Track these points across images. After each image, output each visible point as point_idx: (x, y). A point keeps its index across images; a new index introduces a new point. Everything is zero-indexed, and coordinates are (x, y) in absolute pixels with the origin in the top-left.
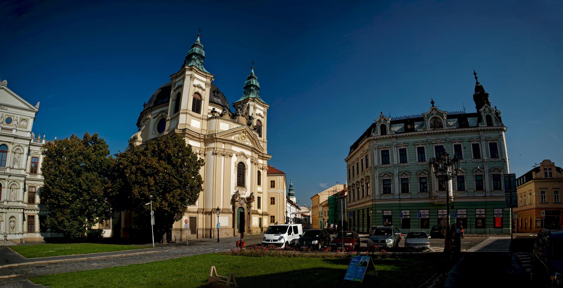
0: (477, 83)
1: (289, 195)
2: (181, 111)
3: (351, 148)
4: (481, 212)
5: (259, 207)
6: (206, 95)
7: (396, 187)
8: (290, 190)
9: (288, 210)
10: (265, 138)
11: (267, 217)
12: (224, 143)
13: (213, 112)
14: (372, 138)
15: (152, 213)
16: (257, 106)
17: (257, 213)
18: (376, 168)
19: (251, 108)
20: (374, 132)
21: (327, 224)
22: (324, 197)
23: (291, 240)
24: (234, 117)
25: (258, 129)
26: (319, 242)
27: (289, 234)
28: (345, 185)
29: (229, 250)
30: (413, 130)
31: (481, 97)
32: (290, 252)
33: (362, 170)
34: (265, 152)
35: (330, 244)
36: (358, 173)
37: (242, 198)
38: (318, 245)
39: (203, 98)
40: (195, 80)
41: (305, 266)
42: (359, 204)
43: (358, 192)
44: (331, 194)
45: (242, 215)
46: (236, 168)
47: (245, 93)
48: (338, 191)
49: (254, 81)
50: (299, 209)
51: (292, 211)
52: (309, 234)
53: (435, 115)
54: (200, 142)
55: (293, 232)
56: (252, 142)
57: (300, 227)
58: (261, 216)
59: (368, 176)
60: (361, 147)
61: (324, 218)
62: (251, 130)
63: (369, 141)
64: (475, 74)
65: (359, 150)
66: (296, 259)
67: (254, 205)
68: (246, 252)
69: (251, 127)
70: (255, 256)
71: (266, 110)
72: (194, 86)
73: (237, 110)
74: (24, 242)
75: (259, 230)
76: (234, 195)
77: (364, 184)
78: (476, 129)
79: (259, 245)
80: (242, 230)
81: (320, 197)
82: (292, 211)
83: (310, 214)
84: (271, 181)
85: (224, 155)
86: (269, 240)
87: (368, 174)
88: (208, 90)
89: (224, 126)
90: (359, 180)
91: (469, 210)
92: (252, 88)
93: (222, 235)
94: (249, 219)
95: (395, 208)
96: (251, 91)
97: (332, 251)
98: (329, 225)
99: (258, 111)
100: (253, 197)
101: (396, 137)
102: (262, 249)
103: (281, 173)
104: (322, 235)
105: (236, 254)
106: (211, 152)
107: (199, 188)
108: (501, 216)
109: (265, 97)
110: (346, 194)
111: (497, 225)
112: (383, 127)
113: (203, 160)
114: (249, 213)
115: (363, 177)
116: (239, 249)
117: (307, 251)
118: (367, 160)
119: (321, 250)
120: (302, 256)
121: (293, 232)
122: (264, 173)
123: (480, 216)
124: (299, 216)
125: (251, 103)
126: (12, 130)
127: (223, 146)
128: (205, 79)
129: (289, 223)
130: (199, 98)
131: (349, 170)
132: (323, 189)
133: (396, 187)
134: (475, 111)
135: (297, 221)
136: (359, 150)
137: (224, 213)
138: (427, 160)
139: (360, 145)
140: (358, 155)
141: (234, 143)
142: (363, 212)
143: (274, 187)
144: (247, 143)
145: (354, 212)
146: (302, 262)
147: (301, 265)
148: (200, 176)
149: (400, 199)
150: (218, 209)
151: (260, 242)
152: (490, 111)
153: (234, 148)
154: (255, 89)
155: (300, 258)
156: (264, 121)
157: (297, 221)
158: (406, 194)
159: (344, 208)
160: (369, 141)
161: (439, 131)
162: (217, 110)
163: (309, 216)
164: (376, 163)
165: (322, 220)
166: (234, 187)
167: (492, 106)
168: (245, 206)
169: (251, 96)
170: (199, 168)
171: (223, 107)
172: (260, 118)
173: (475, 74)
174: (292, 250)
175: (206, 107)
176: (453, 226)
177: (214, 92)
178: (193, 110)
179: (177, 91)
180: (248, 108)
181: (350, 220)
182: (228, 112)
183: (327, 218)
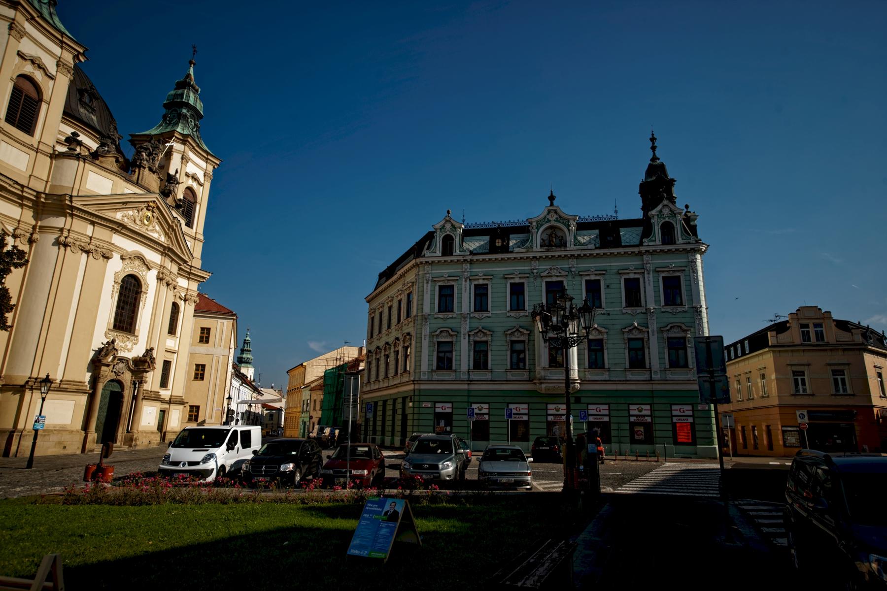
0: (654, 158)
1: (240, 361)
3: (381, 276)
4: (640, 411)
5: (164, 384)
6: (56, 92)
7: (463, 356)
8: (243, 351)
9: (234, 395)
10: (201, 230)
11: (181, 407)
12: (93, 223)
13: (72, 140)
14: (423, 260)
16: (191, 155)
17: (157, 398)
18: (425, 318)
19: (176, 159)
20: (428, 249)
21: (317, 426)
22: (315, 370)
23: (232, 461)
24: (128, 168)
25: (187, 208)
26: (297, 466)
27: (230, 447)
28: (361, 349)
29: (58, 489)
30: (505, 249)
31: (657, 186)
32: (227, 491)
33: (399, 320)
34: (197, 263)
35: (321, 471)
36: (389, 327)
37: (121, 360)
38: (293, 473)
39: (46, 97)
41: (259, 524)
42: (387, 388)
43: (387, 364)
44: (332, 365)
45: (115, 400)
46: (117, 288)
47: (165, 117)
48: (346, 359)
49: (192, 95)
50: (259, 393)
51: (241, 398)
52: (277, 448)
53: (553, 223)
54: (22, 206)
55: (239, 444)
56: (166, 234)
57: (256, 432)
58: (166, 406)
59: (408, 334)
60: (401, 276)
61: (313, 413)
62: (169, 206)
63: (416, 265)
64: (653, 139)
65: (395, 281)
66: (239, 507)
67: (152, 380)
68: (110, 493)
69: (170, 200)
70: (133, 504)
71: (210, 169)
72: (20, 55)
73: (139, 153)
75: (157, 438)
76: (101, 350)
77: (400, 348)
78: (636, 250)
79: (149, 474)
80: (108, 435)
81: (308, 369)
82: (241, 398)
83: (282, 404)
84: (203, 329)
85: (88, 252)
86: (177, 463)
87: (410, 329)
88: (63, 82)
89: (99, 182)
90: (391, 340)
91: (613, 407)
92: (184, 111)
93: (46, 448)
94: (135, 411)
95: (458, 399)
96: (180, 117)
97: (323, 487)
98: (321, 430)
99: (191, 168)
100: (153, 360)
101: (471, 262)
102: (155, 484)
103: (226, 313)
105: (77, 501)
106: (52, 237)
108: (691, 420)
110: (362, 366)
111: (682, 437)
112: (448, 242)
113: (21, 254)
114: (135, 398)
115: (399, 336)
116: (91, 485)
117: (266, 488)
118: (409, 302)
119: (299, 486)
120: (254, 501)
121: (239, 444)
122: (187, 311)
123: (640, 420)
124: (257, 409)
125: (177, 146)
127: (89, 230)
128: (57, 50)
129: (233, 423)
131: (373, 319)
132: (316, 355)
133: (463, 356)
134: (639, 215)
135: (251, 418)
136: (395, 281)
137: (65, 391)
138: (528, 307)
139: (399, 273)
140: (392, 292)
141: (119, 228)
142: (394, 404)
143: (207, 342)
144: (155, 236)
145: (376, 403)
146: (254, 514)
147: (249, 523)
148: (5, 291)
149: (470, 382)
150: (47, 380)
151: (153, 468)
152: (673, 214)
153: (119, 240)
154: (192, 116)
155: (249, 506)
156: (203, 194)
157: (251, 418)
158: (482, 372)
159: (355, 395)
160: (416, 265)
161: (556, 254)
162: (82, 138)
163: (280, 410)
164: (427, 310)
165: (306, 420)
166: (105, 329)
167: (680, 205)
169: (179, 129)
170: (8, 271)
171: (103, 137)
172: (195, 185)
173: (653, 139)
174: (233, 486)
175: (52, 125)
176: (580, 437)
177: (81, 92)
178: (10, 119)
180: (169, 154)
181: (367, 420)
182: (113, 152)
183: (317, 415)
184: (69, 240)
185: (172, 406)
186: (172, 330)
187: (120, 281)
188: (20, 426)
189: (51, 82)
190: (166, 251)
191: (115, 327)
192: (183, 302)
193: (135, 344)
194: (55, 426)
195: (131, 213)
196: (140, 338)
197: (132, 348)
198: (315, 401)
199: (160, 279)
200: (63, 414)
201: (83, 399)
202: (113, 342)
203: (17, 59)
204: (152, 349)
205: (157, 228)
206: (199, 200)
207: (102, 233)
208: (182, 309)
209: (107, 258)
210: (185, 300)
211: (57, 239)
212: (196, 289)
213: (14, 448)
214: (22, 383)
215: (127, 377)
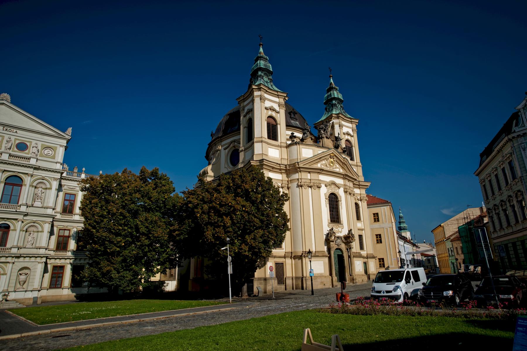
1: (400, 229)
2: (255, 140)
3: (482, 155)
5: (362, 248)
6: (281, 118)
8: (400, 223)
9: (402, 250)
10: (359, 160)
11: (374, 260)
12: (309, 172)
13: (292, 137)
14: (515, 135)
15: (229, 259)
16: (343, 123)
17: (360, 256)
19: (337, 127)
20: (517, 125)
21: (462, 265)
22: (451, 228)
23: (411, 290)
24: (317, 140)
25: (348, 151)
26: (454, 293)
27: (407, 282)
28: (481, 209)
29: (327, 306)
32: (412, 308)
33: (507, 183)
34: (362, 179)
35: (475, 296)
36: (500, 189)
37: (338, 237)
38: (453, 298)
39: (278, 122)
40: (266, 102)
41: (437, 329)
42: (512, 233)
43: (507, 216)
44: (462, 223)
45: (340, 258)
46: (327, 201)
47: (326, 109)
48: (472, 217)
49: (335, 92)
50: (417, 247)
51: (407, 251)
52: (437, 282)
54: (281, 173)
55: (412, 280)
56: (342, 168)
57: (421, 271)
59: (519, 191)
60: (499, 152)
61: (457, 257)
62: (340, 153)
63: (510, 140)
65: (495, 156)
66: (422, 318)
67: (355, 246)
68: (350, 308)
69: (340, 150)
70: (363, 315)
71: (354, 126)
72: (266, 108)
73: (320, 131)
74: (39, 302)
75: (365, 278)
76: (328, 234)
77: (515, 202)
79: (366, 298)
80: (342, 278)
82: (407, 251)
83: (434, 252)
84: (374, 214)
85: (311, 187)
86: (379, 292)
87: (520, 187)
88: (283, 112)
89: (307, 152)
90: (504, 198)
92: (334, 102)
93: (317, 286)
94: (351, 264)
96: (333, 106)
97: (479, 306)
98: (467, 268)
99: (345, 130)
102: (371, 303)
103: (385, 203)
104: (460, 282)
105: (336, 312)
106: (295, 184)
107: (285, 228)
109: (351, 111)
110: (486, 220)
113: (286, 194)
114: (349, 257)
115: (511, 193)
116: (341, 304)
117: (437, 307)
118: (512, 169)
119: (460, 306)
120: (431, 315)
121: (412, 280)
122: (363, 205)
124: (418, 257)
125: (335, 121)
126: (29, 159)
127: (309, 176)
128: (277, 100)
129: (406, 267)
130: (274, 123)
131: (484, 186)
132: (449, 217)
135: (417, 263)
136: (495, 156)
137: (318, 256)
139: (496, 150)
140: (494, 164)
141: (321, 171)
143: (378, 221)
145: (506, 245)
146: (433, 323)
147: (431, 329)
148: (285, 213)
150: (310, 252)
151: (368, 295)
153: (322, 177)
154: (338, 103)
155: (429, 318)
156: (354, 141)
157: (417, 263)
160: (510, 140)
162: (296, 134)
163: (433, 256)
165: (454, 261)
168: (343, 247)
169: (334, 112)
170: (283, 204)
171: (303, 130)
172: (349, 138)
174: (415, 305)
175: (283, 133)
177: (290, 113)
179: (248, 117)
180: (333, 127)
181: (502, 259)
182: (309, 136)
183: (461, 257)
184: (302, 183)
185: (369, 260)
186: (358, 218)
188: (305, 275)
189: (279, 114)
190: (345, 177)
192: (360, 202)
194: (318, 274)
195: (324, 162)
196: (344, 225)
197: (342, 231)
198: (456, 248)
199: (346, 192)
200: (319, 267)
201: (327, 259)
202: (332, 229)
203: (265, 111)
204: (351, 230)
205: (338, 166)
206: (353, 145)
207: (314, 176)
208: (360, 205)
209: (319, 187)
210: (361, 200)
211: (298, 184)
212: (365, 193)
213: (305, 285)
214: (301, 254)
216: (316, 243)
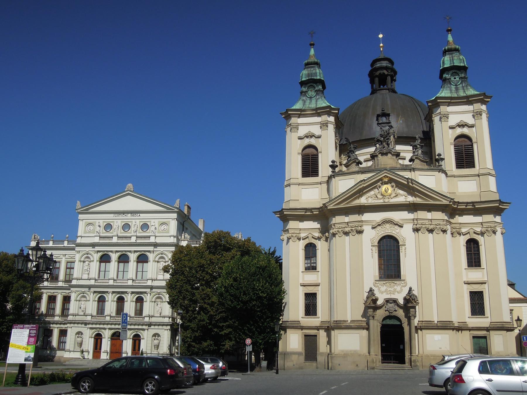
46: (376, 250)
126: (149, 237)
153: (367, 216)
168: (400, 313)
185: (491, 332)
187: (376, 244)
191: (380, 278)
193: (404, 286)
194: (351, 351)
195: (372, 193)
199: (416, 230)
205: (401, 192)
215: (400, 313)
216: (351, 310)
